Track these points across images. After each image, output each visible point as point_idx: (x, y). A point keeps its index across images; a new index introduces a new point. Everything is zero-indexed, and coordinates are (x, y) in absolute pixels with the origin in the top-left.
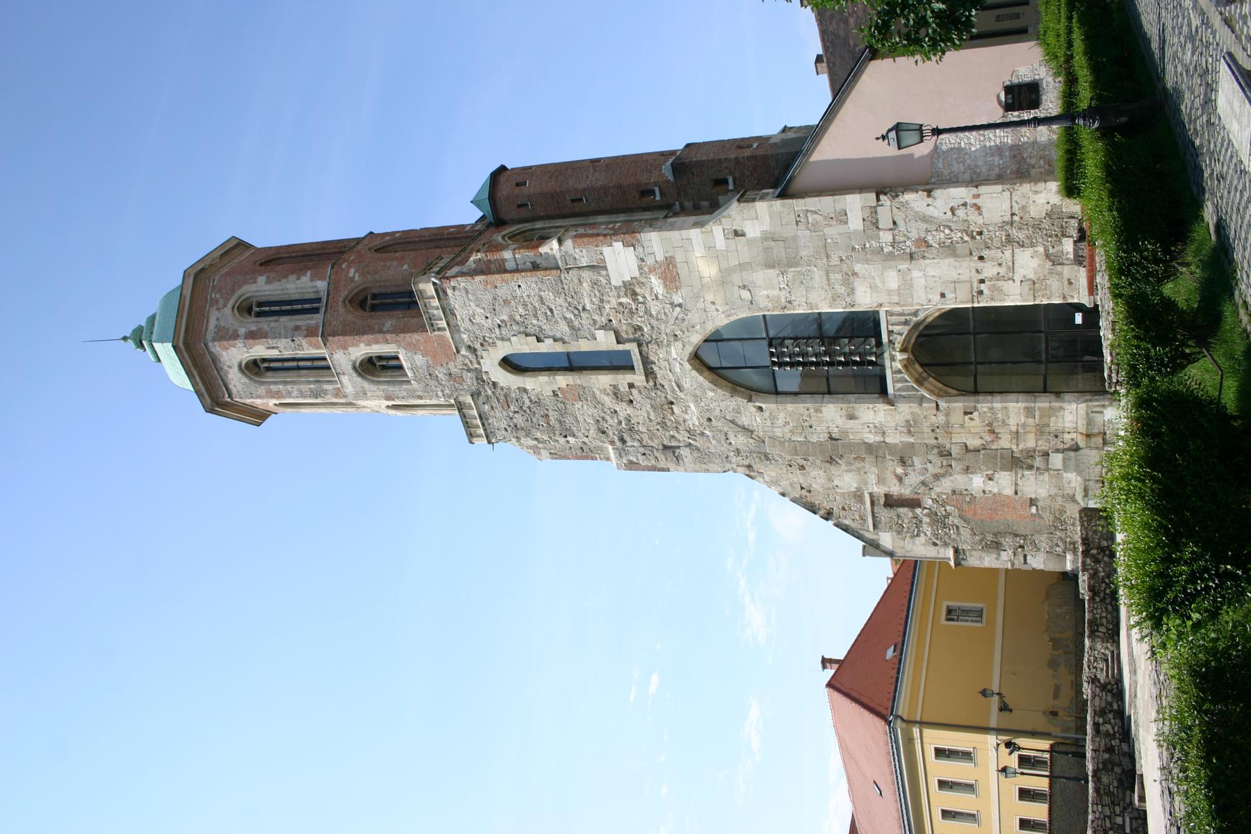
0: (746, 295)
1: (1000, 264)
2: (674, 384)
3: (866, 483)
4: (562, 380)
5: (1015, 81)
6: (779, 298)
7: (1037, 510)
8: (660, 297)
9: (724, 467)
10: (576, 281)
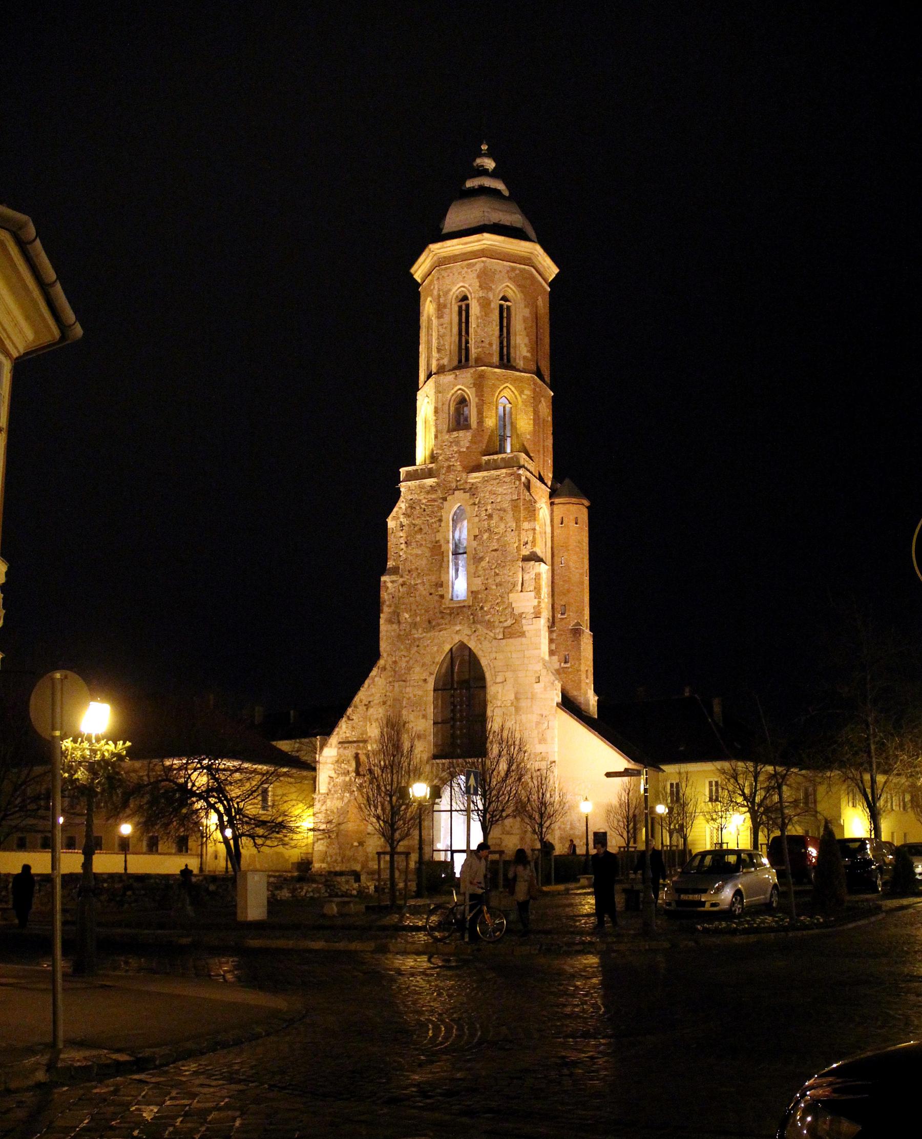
1: (511, 827)
5: (608, 837)
6: (497, 699)
7: (356, 846)
8: (501, 625)
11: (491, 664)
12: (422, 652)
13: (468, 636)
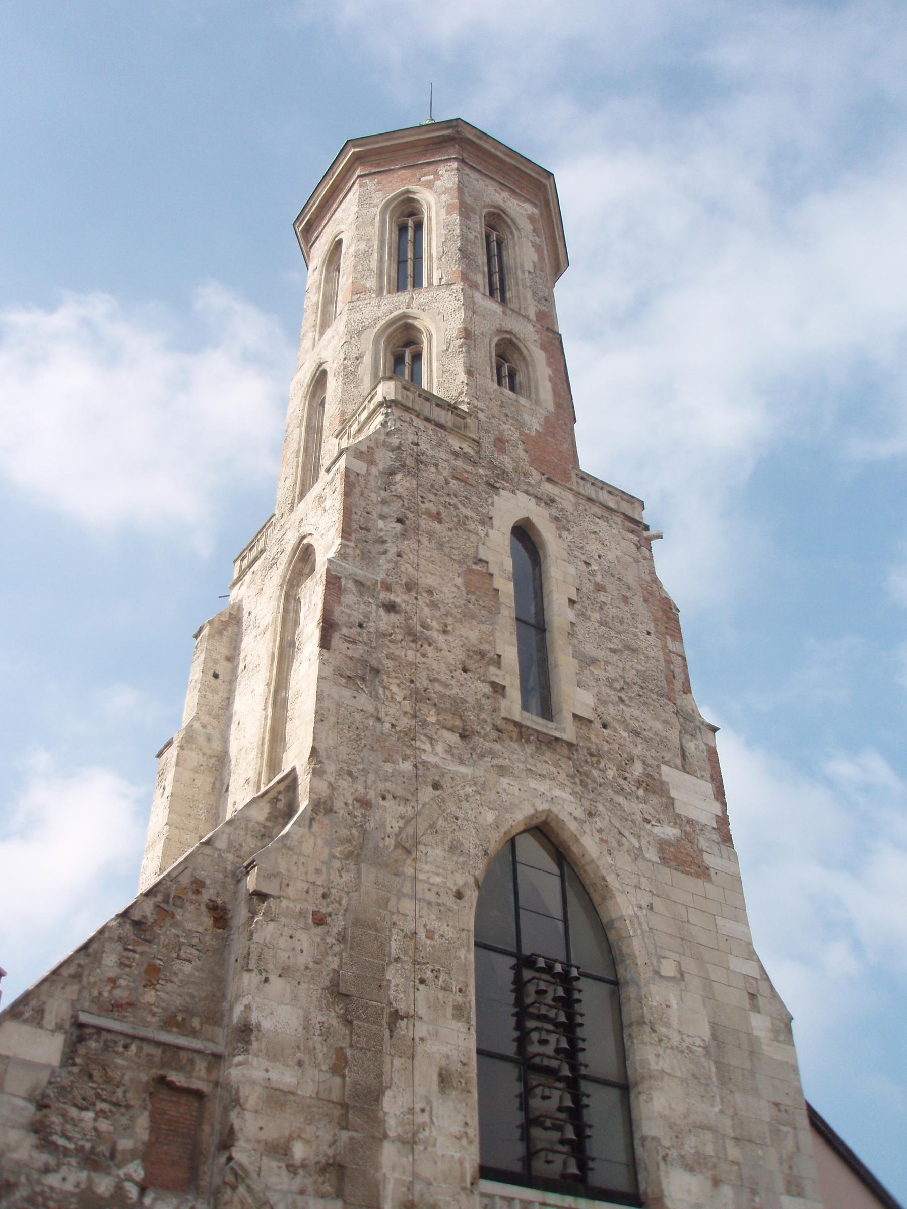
0: (668, 968)
2: (507, 762)
3: (274, 1055)
4: (506, 588)
8: (648, 826)
9: (328, 758)
10: (665, 716)
11: (643, 920)
12: (452, 808)
13: (575, 818)
